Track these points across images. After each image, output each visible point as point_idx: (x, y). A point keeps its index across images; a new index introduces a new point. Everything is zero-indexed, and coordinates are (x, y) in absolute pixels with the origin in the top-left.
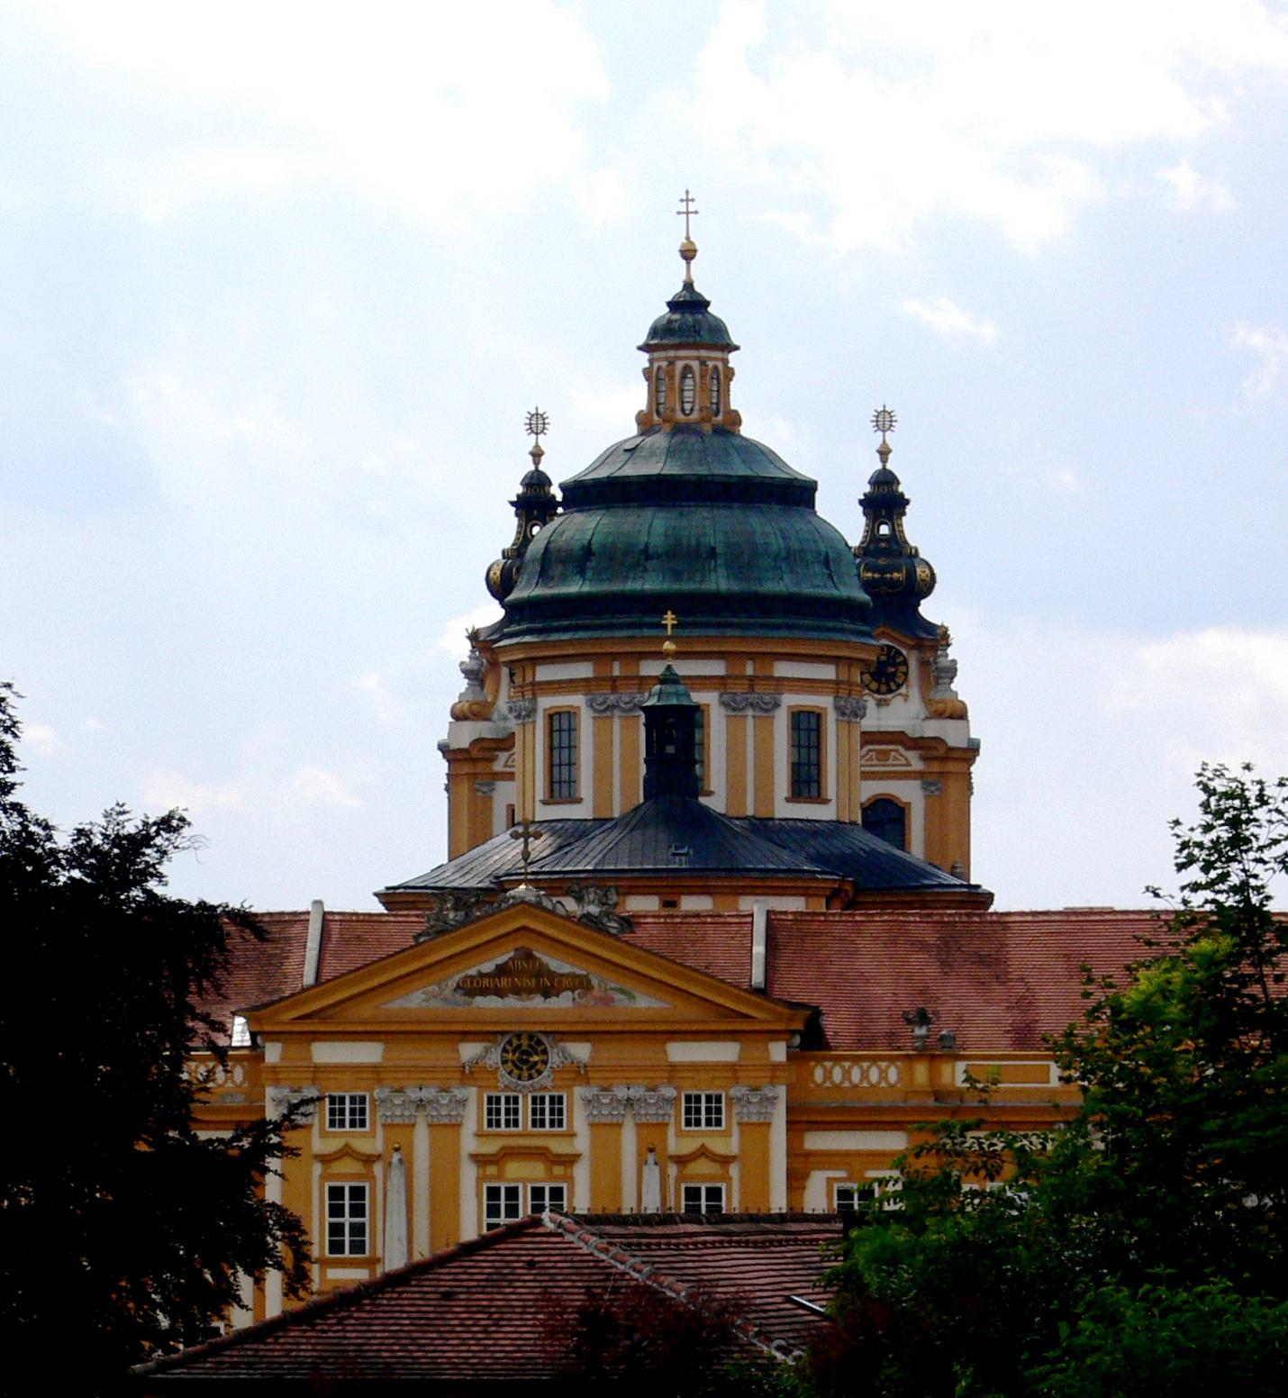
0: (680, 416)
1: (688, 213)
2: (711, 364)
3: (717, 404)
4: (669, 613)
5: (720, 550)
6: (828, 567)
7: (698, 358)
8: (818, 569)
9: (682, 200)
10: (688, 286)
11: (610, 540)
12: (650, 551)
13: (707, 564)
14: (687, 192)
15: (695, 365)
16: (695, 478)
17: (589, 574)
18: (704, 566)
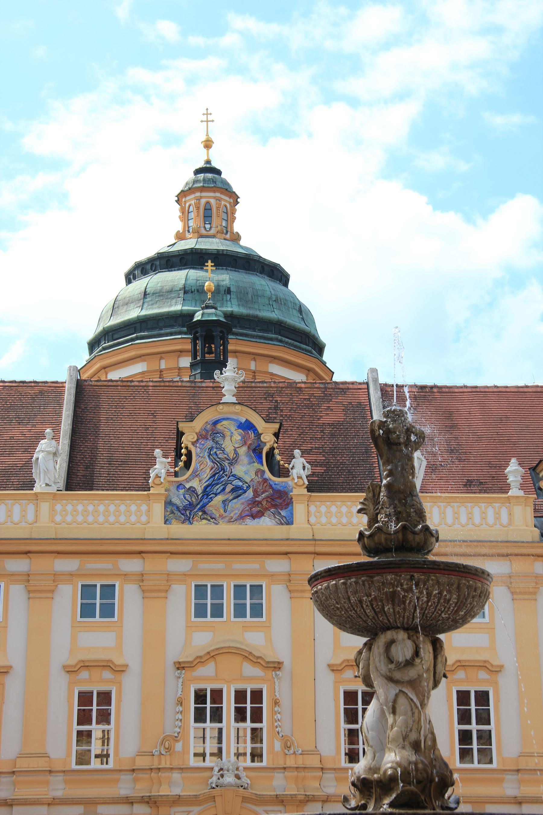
0: (203, 232)
1: (207, 121)
2: (223, 203)
3: (227, 228)
4: (210, 261)
5: (232, 289)
6: (301, 314)
7: (214, 198)
8: (296, 313)
9: (204, 114)
10: (208, 162)
11: (159, 285)
12: (187, 289)
13: (225, 297)
14: (207, 109)
15: (213, 201)
16: (215, 252)
17: (145, 306)
18: (223, 299)
